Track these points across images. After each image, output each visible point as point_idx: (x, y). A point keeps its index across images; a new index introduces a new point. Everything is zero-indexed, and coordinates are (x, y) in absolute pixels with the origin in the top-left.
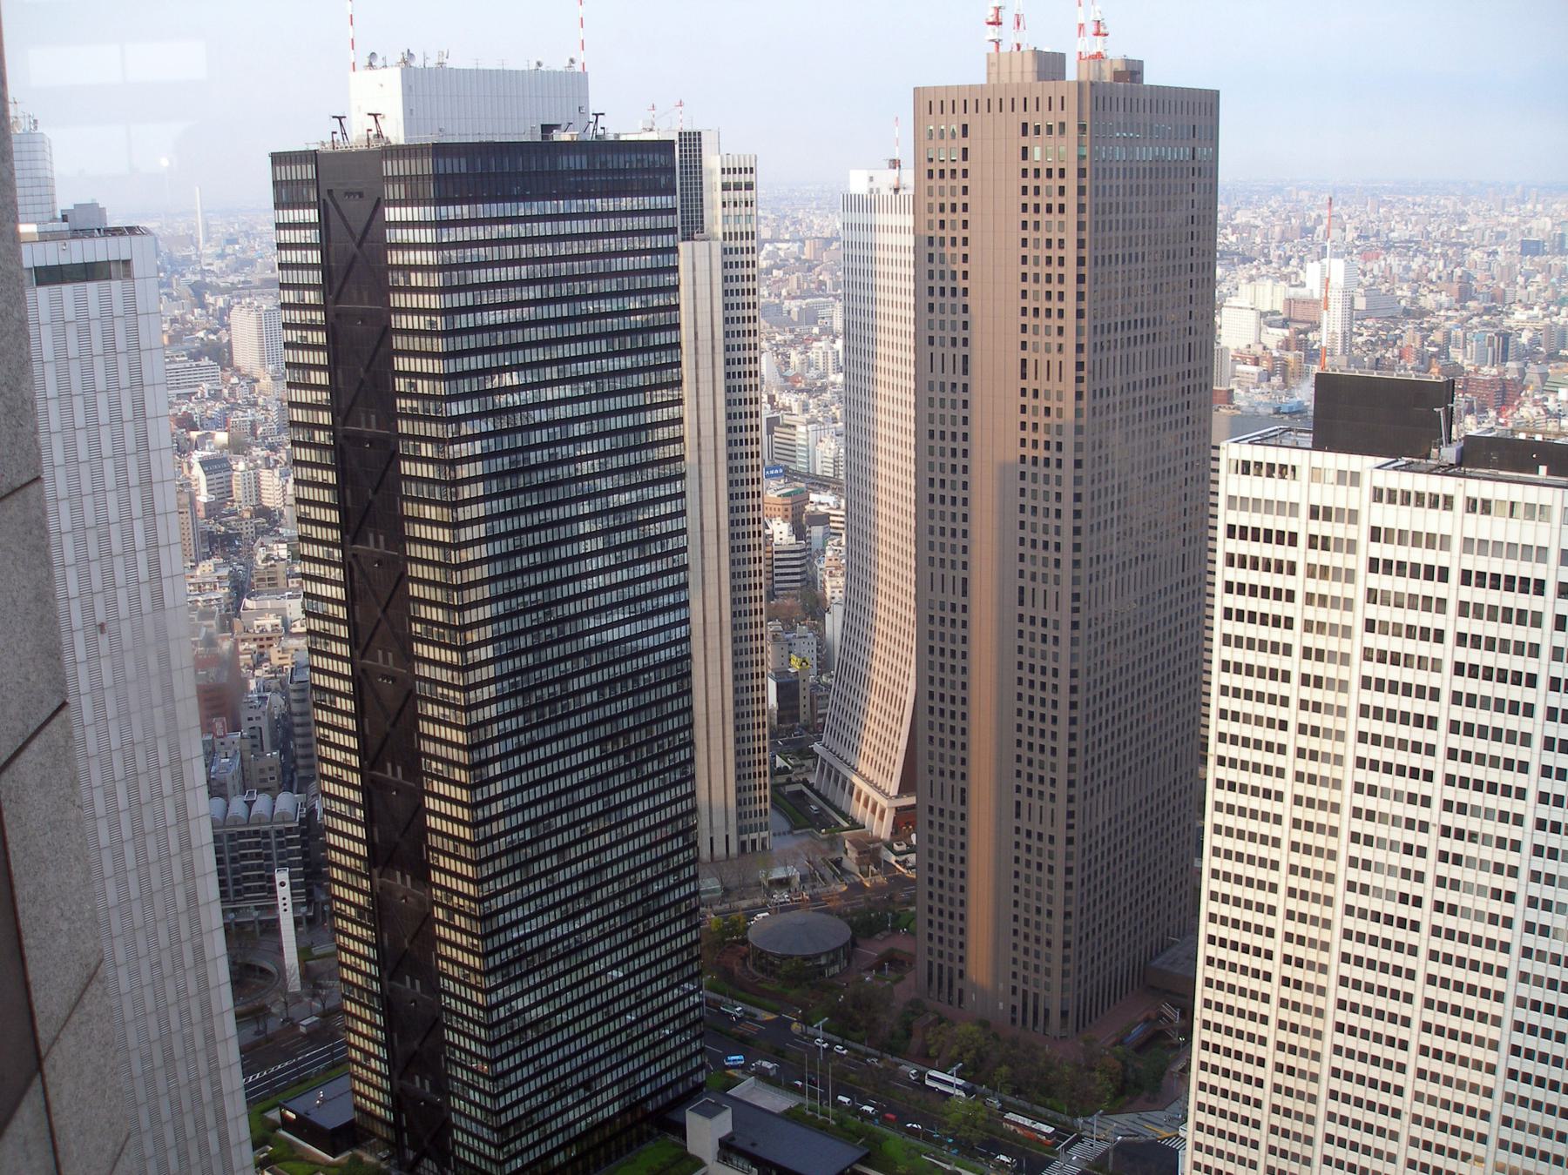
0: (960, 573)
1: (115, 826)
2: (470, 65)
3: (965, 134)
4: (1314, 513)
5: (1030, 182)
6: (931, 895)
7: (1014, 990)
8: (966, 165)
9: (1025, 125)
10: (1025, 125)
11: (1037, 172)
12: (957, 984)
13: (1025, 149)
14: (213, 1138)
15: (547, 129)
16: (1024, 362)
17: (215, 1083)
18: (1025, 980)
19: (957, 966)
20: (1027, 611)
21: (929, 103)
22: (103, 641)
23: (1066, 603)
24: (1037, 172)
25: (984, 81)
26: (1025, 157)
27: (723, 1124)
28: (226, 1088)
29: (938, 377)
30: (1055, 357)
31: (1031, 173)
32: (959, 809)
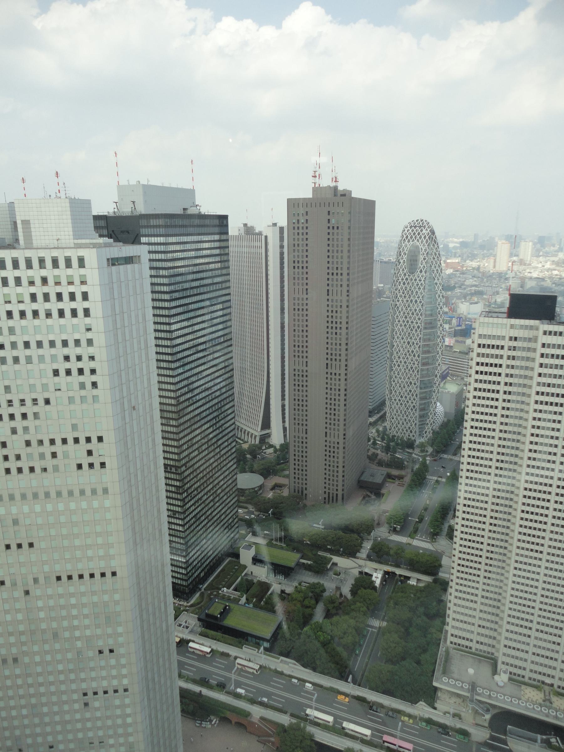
0: (305, 360)
1: (137, 488)
2: (159, 184)
3: (307, 214)
4: (511, 339)
5: (331, 231)
6: (295, 464)
7: (325, 492)
8: (307, 225)
9: (329, 212)
10: (329, 212)
11: (333, 227)
12: (305, 492)
13: (329, 220)
14: (163, 605)
15: (184, 209)
16: (328, 290)
17: (164, 582)
18: (329, 489)
19: (304, 486)
20: (329, 371)
21: (293, 204)
22: (134, 413)
23: (343, 367)
24: (333, 227)
25: (310, 196)
26: (329, 222)
27: (252, 552)
28: (167, 584)
29: (297, 296)
30: (339, 289)
31: (331, 228)
32: (305, 436)
